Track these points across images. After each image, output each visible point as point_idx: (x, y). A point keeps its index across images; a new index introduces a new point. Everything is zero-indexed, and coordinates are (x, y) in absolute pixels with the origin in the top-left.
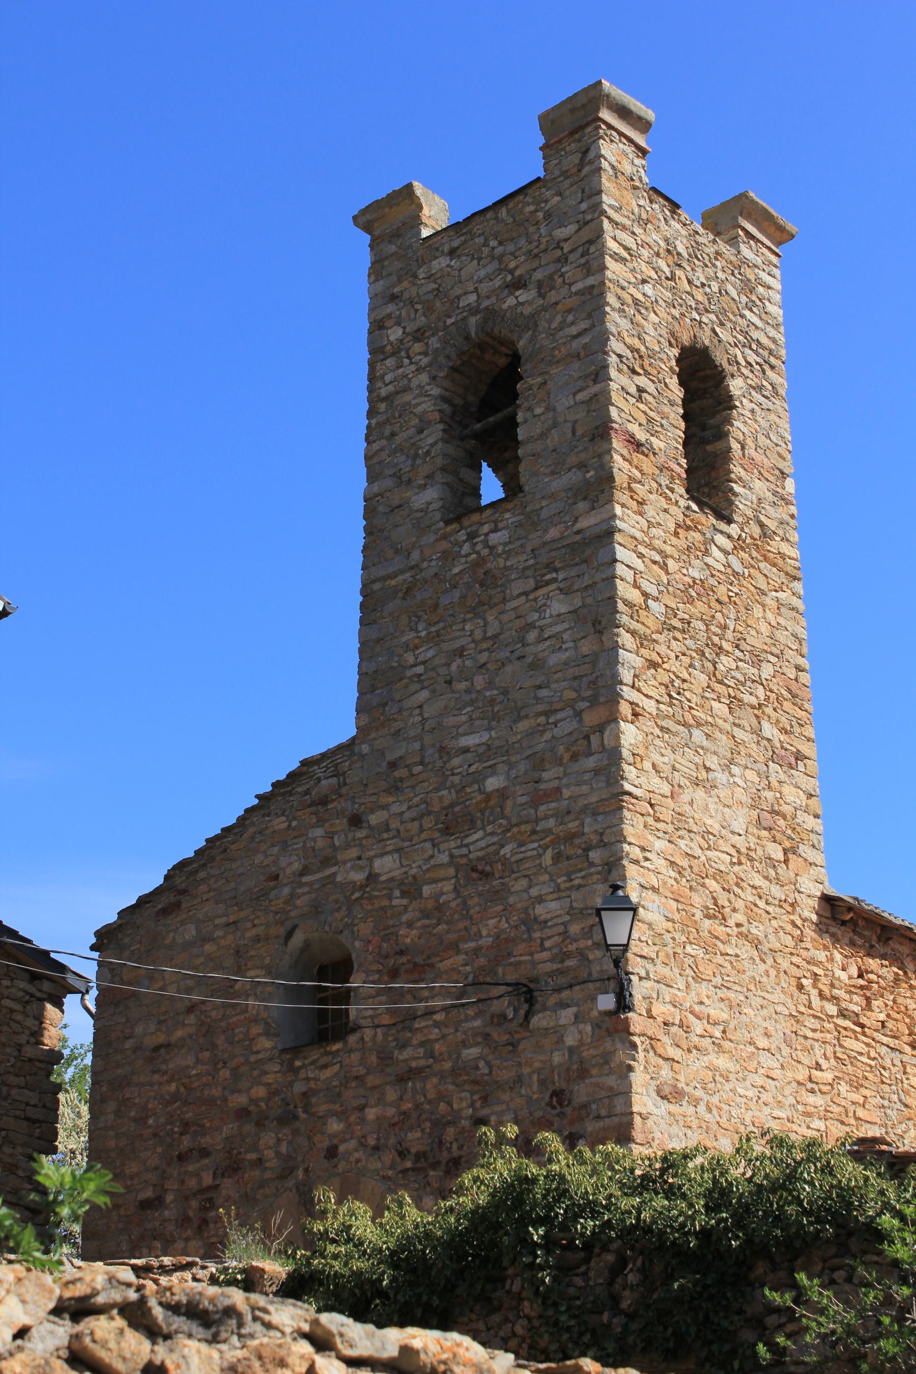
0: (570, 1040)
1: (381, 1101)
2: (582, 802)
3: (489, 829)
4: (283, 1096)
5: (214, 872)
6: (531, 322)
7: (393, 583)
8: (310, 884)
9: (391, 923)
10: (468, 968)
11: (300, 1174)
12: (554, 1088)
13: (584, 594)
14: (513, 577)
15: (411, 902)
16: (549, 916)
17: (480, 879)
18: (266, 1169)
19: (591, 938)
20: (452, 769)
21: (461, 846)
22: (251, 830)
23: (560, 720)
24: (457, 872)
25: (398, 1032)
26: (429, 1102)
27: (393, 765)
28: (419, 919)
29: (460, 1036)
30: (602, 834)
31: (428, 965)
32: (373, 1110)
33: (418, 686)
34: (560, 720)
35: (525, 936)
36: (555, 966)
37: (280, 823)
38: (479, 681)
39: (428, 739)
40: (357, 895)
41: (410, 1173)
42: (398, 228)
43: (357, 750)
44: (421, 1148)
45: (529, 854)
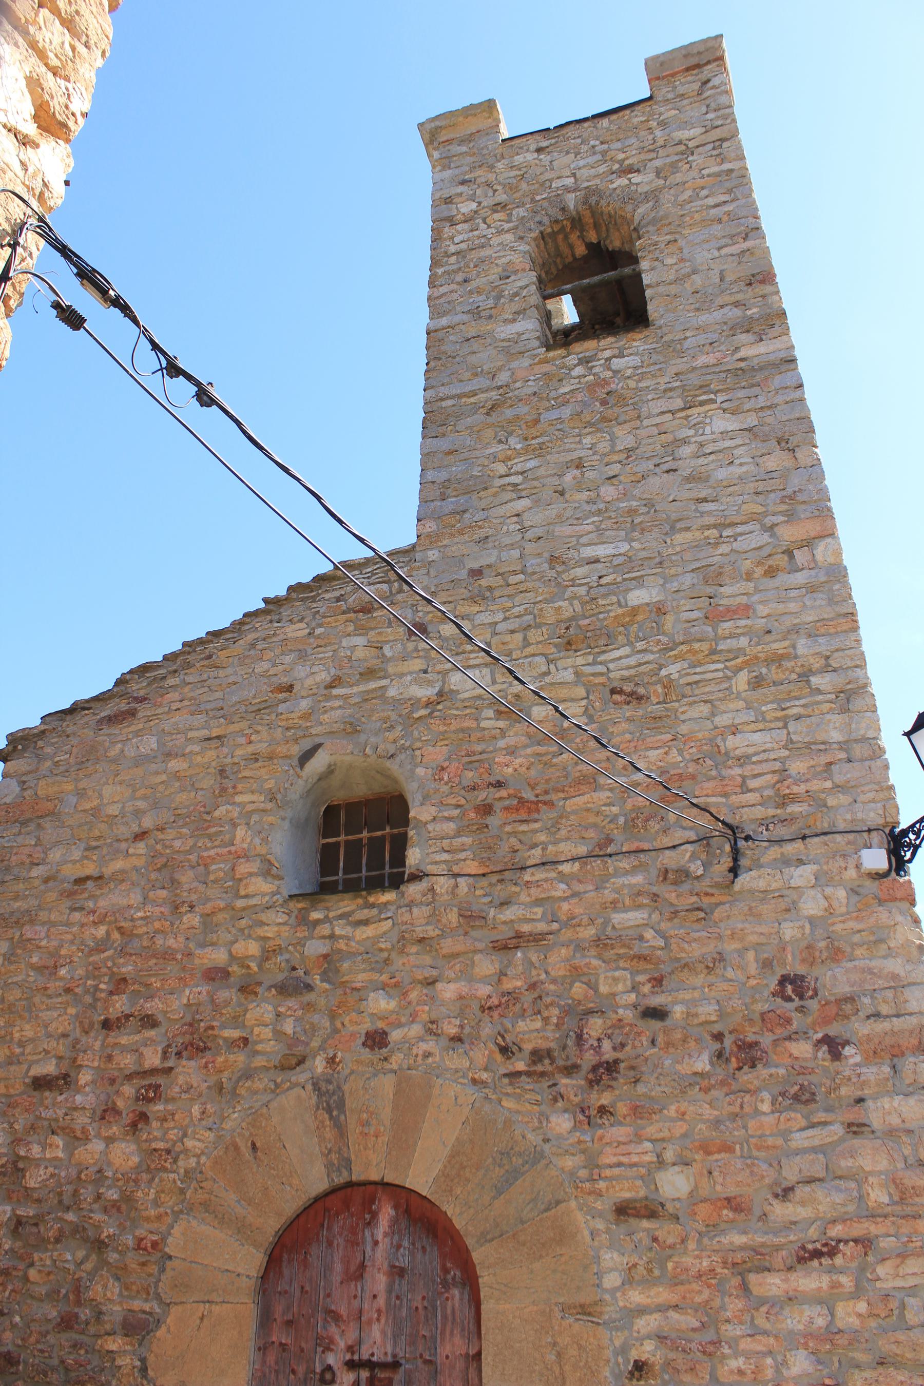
0: (812, 905)
1: (466, 975)
2: (788, 622)
3: (640, 645)
4: (287, 956)
5: (189, 679)
6: (653, 196)
7: (472, 400)
8: (345, 697)
9: (479, 748)
10: (615, 810)
11: (319, 1065)
12: (784, 972)
13: (760, 414)
14: (650, 397)
15: (511, 726)
16: (751, 750)
17: (628, 703)
18: (256, 1053)
19: (830, 777)
20: (573, 580)
21: (595, 663)
22: (251, 637)
23: (741, 534)
24: (588, 693)
25: (491, 885)
26: (554, 981)
27: (477, 573)
28: (526, 746)
29: (608, 895)
30: (827, 658)
31: (545, 803)
32: (452, 986)
33: (514, 496)
34: (741, 534)
35: (714, 773)
36: (771, 812)
37: (297, 631)
38: (608, 492)
39: (530, 548)
40: (423, 712)
41: (523, 1078)
42: (472, 134)
43: (418, 556)
44: (543, 1044)
45: (709, 676)
